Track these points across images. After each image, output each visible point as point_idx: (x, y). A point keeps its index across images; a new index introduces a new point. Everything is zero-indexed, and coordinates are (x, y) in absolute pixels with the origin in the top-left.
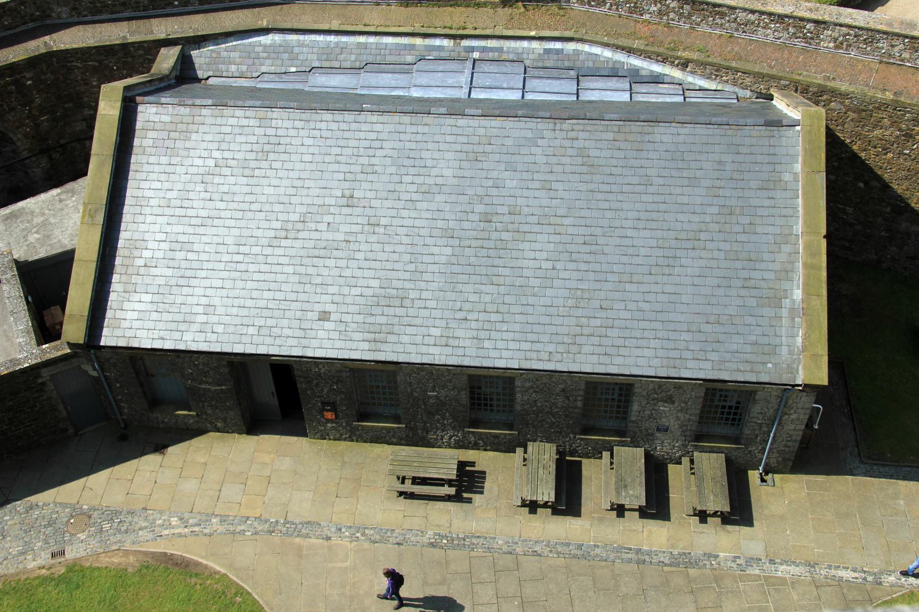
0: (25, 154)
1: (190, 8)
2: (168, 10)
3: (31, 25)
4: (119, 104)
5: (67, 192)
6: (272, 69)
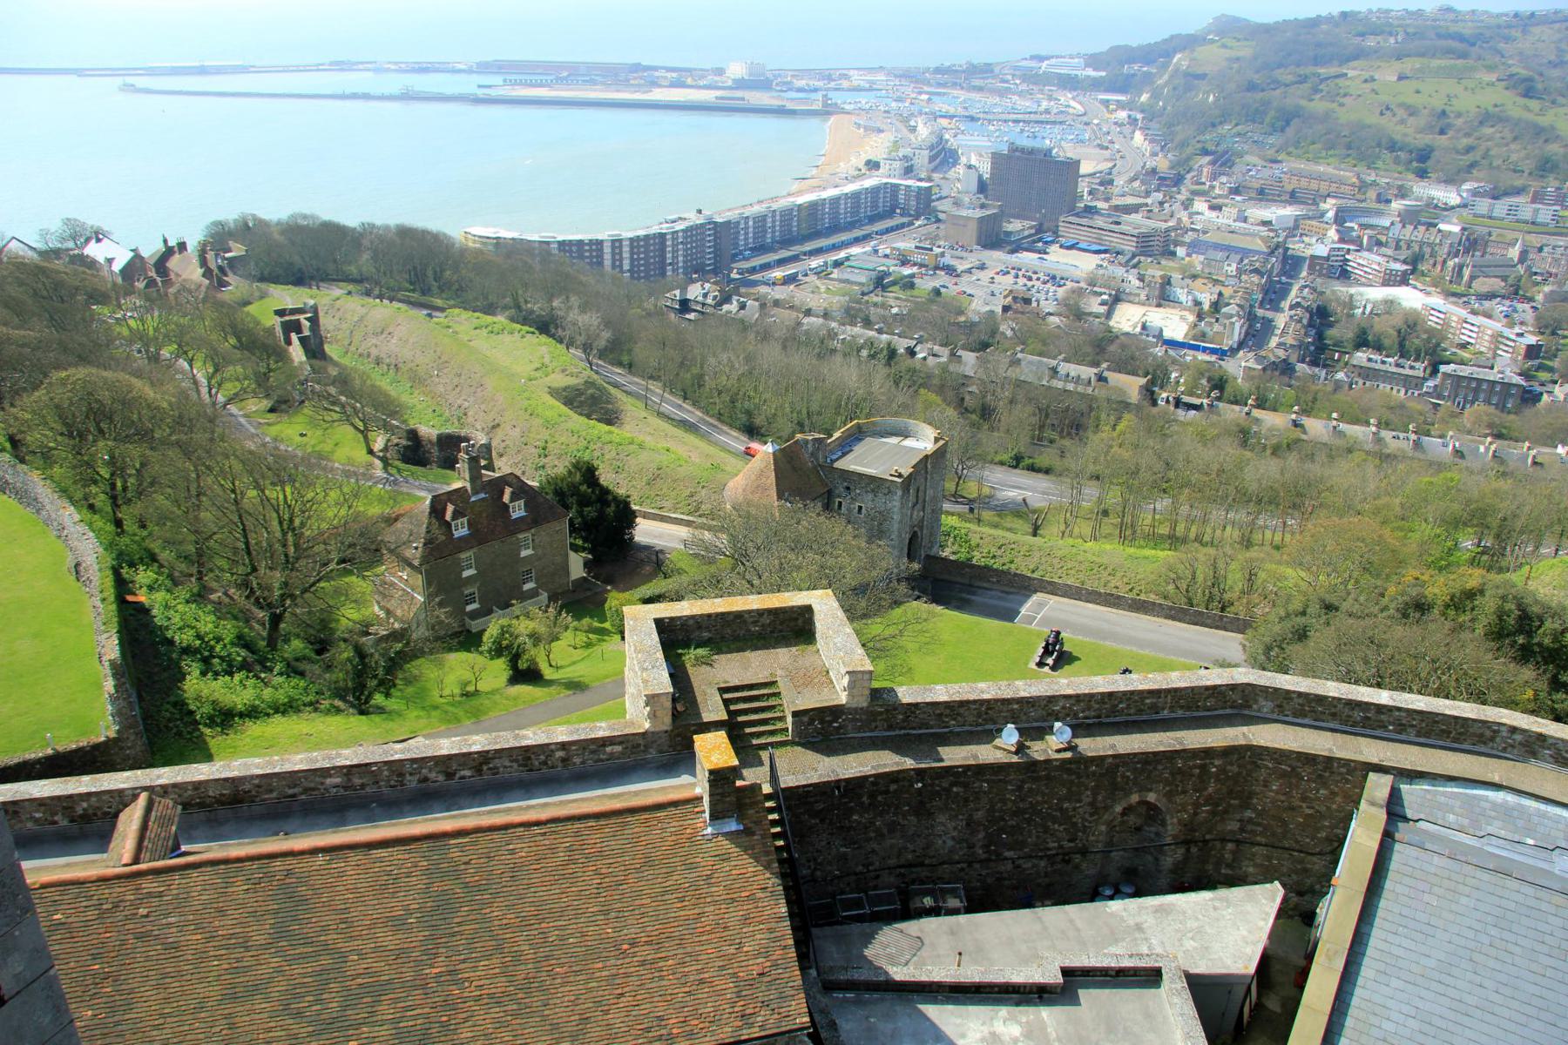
0: (1169, 840)
1: (1403, 737)
2: (1377, 733)
3: (1228, 711)
4: (1378, 837)
5: (1221, 899)
6: (1503, 833)
